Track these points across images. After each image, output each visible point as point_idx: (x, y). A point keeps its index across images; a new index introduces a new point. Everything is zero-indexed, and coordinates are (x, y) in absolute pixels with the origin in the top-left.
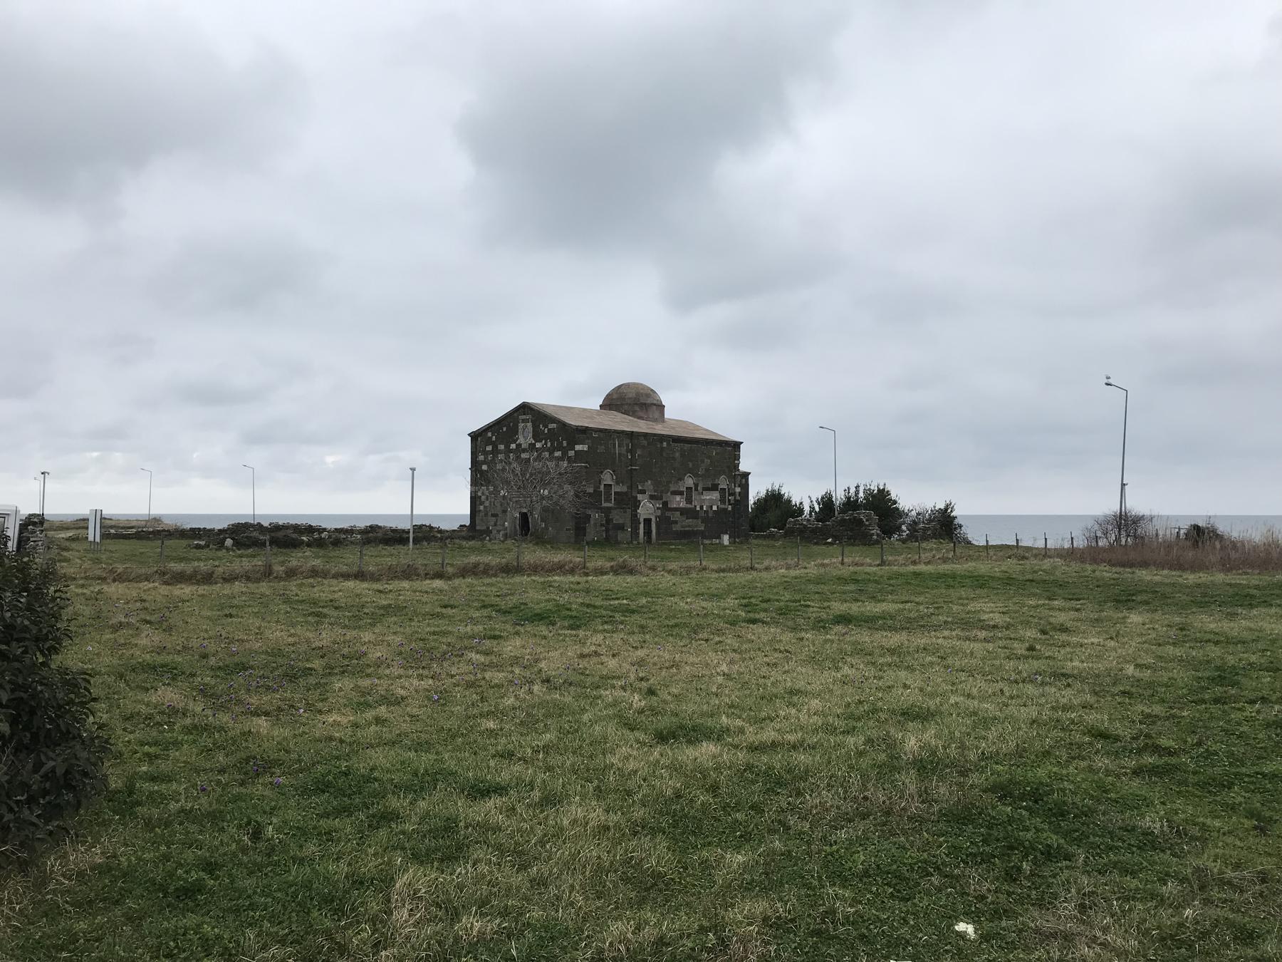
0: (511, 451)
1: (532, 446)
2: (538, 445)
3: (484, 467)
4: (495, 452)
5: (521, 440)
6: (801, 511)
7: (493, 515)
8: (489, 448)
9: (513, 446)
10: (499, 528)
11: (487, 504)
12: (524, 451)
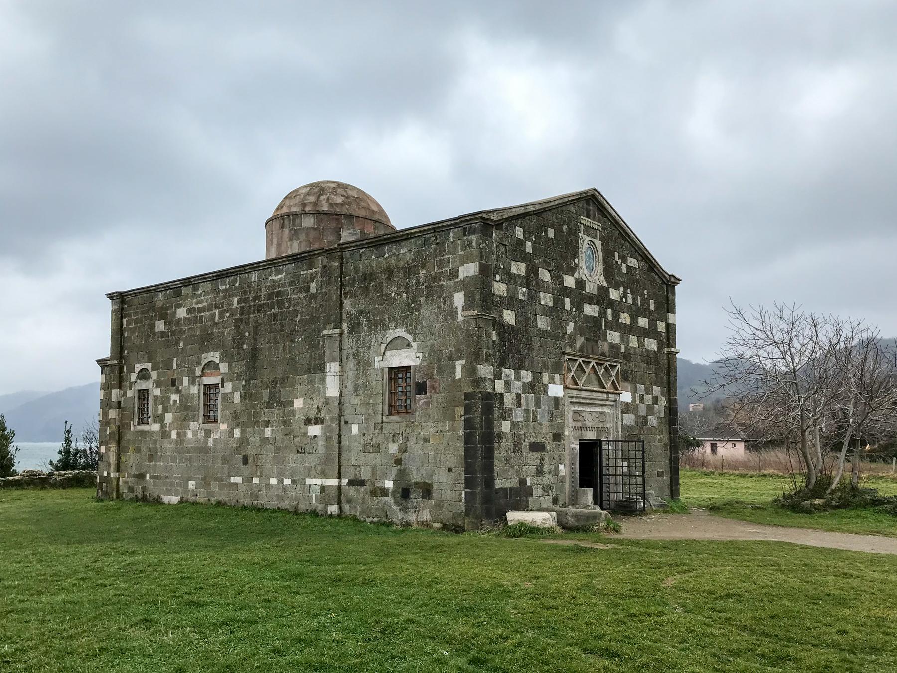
0: (566, 291)
1: (603, 292)
2: (614, 295)
3: (509, 317)
4: (531, 280)
7: (537, 447)
8: (519, 268)
9: (569, 281)
10: (546, 479)
11: (519, 415)
12: (590, 299)
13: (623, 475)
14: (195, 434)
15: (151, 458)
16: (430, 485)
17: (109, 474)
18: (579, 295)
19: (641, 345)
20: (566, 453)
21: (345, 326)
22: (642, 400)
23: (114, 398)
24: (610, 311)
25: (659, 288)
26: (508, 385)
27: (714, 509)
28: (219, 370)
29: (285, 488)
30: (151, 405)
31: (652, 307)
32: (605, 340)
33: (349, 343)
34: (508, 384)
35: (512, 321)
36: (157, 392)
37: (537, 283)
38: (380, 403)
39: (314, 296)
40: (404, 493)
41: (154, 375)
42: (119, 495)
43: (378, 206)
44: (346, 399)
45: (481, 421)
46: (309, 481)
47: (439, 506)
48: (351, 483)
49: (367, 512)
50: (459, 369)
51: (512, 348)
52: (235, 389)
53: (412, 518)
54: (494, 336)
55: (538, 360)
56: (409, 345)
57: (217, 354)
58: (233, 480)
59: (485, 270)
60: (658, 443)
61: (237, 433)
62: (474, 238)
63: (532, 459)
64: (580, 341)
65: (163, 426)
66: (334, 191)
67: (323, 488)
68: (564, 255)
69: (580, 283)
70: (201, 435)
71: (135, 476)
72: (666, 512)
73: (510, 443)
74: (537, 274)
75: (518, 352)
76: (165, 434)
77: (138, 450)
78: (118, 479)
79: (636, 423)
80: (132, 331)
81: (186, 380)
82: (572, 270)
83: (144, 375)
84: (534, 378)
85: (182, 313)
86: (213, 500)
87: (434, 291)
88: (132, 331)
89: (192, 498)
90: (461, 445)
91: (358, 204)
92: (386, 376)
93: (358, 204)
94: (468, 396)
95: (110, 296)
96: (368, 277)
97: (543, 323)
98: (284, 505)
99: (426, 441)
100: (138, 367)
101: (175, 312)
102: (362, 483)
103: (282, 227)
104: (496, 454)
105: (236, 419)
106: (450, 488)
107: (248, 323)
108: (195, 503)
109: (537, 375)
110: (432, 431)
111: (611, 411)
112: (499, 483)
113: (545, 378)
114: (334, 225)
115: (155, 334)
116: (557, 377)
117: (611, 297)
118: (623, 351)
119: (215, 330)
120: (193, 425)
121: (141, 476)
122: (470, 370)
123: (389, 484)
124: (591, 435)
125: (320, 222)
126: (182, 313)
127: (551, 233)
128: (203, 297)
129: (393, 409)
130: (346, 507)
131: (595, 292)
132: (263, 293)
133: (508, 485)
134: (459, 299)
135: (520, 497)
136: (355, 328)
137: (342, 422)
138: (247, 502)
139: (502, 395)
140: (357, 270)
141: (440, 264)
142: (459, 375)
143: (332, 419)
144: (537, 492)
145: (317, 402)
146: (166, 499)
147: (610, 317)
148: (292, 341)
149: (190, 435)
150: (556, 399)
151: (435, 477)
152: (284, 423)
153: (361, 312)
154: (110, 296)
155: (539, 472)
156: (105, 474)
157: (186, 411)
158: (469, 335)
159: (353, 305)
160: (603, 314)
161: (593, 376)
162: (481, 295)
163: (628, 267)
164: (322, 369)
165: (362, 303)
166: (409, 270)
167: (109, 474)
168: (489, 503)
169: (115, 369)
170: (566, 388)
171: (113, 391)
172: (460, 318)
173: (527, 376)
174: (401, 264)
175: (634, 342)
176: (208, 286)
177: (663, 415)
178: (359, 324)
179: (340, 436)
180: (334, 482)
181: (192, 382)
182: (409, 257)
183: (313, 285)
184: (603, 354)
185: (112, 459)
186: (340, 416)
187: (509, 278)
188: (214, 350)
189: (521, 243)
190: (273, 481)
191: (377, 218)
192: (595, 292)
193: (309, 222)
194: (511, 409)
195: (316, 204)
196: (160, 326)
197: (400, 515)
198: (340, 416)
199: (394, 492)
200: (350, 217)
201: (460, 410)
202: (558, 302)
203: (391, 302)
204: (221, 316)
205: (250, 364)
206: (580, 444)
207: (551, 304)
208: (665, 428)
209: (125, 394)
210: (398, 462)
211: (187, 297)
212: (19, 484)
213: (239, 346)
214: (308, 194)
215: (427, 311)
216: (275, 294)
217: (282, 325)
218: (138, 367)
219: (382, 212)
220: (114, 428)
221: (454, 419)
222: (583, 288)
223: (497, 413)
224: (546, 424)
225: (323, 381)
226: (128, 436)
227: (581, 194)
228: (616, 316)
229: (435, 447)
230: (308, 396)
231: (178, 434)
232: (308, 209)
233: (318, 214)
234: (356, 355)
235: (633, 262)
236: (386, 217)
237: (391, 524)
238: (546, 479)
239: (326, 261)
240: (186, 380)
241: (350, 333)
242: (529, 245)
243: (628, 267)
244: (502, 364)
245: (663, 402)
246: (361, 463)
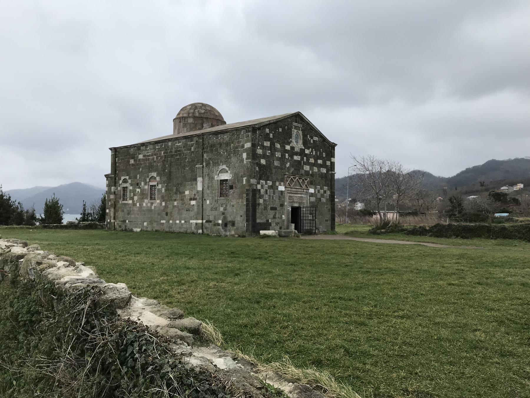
0: (287, 151)
1: (302, 151)
2: (307, 152)
3: (263, 162)
4: (272, 148)
5: (294, 144)
6: (32, 217)
7: (273, 209)
8: (267, 144)
9: (288, 147)
10: (277, 220)
11: (266, 197)
12: (297, 154)
13: (310, 220)
14: (147, 204)
15: (129, 214)
16: (234, 222)
17: (110, 221)
18: (292, 152)
19: (319, 170)
20: (286, 211)
21: (204, 164)
22: (319, 192)
23: (112, 190)
24: (305, 158)
25: (327, 148)
26: (262, 186)
27: (346, 234)
28: (156, 179)
29: (182, 224)
30: (128, 193)
31: (324, 156)
32: (303, 169)
33: (206, 170)
34: (263, 186)
35: (264, 163)
36: (131, 188)
37: (275, 149)
38: (217, 192)
39: (193, 152)
40: (225, 225)
41: (130, 181)
42: (115, 229)
43: (218, 113)
44: (204, 191)
45: (252, 198)
46: (191, 221)
47: (237, 229)
48: (207, 222)
49: (212, 232)
50: (244, 181)
51: (264, 173)
52: (162, 187)
53: (228, 233)
54: (257, 169)
55: (274, 177)
56: (227, 172)
57: (156, 173)
58: (162, 222)
59: (254, 145)
60: (326, 209)
61: (164, 204)
62: (249, 133)
63: (271, 213)
64: (292, 170)
65: (133, 201)
66: (201, 108)
67: (196, 224)
68: (286, 137)
69: (293, 148)
70: (149, 205)
71: (122, 221)
72: (325, 234)
73: (263, 207)
74: (274, 145)
75: (266, 174)
76: (134, 204)
77: (123, 211)
78: (114, 223)
79: (316, 201)
80: (120, 163)
81: (143, 183)
82: (289, 143)
83: (125, 181)
84: (272, 183)
85: (141, 157)
86: (154, 230)
87: (236, 152)
88: (120, 163)
89: (145, 229)
90: (245, 207)
91: (210, 113)
92: (219, 183)
93: (210, 113)
94: (247, 190)
95: (111, 149)
96: (213, 146)
97: (276, 163)
98: (182, 230)
99: (233, 206)
100: (123, 178)
101: (138, 157)
102: (211, 222)
103: (180, 122)
104: (257, 211)
105: (163, 199)
106: (241, 222)
107: (167, 162)
108: (146, 231)
109: (274, 183)
110: (235, 203)
111: (306, 195)
112: (258, 221)
113: (277, 183)
114: (200, 122)
115: (130, 165)
116: (282, 183)
117: (306, 152)
118: (311, 173)
119: (155, 164)
120: (146, 201)
121: (124, 221)
122: (248, 181)
123: (220, 222)
124: (296, 205)
125: (195, 120)
126: (141, 157)
127: (280, 130)
128: (150, 151)
129: (221, 195)
130: (205, 231)
131: (299, 151)
132: (173, 150)
133: (262, 222)
134: (245, 155)
135: (267, 226)
136: (208, 165)
137: (203, 200)
138: (167, 230)
140: (208, 142)
141: (238, 142)
142: (244, 183)
143: (199, 199)
144: (273, 225)
145: (194, 192)
146: (135, 230)
147: (305, 160)
148: (185, 169)
149: (144, 205)
150: (282, 191)
151: (236, 219)
152: (182, 200)
153: (210, 159)
154: (111, 149)
155: (274, 217)
156: (109, 221)
157: (143, 195)
158: (248, 169)
159: (207, 156)
160: (302, 159)
161: (297, 183)
162: (253, 155)
163: (314, 141)
164: (196, 180)
165: (210, 155)
166: (228, 144)
167: (110, 221)
168: (255, 227)
169: (113, 179)
170: (285, 187)
171: (112, 188)
172: (245, 162)
173: (270, 183)
174: (225, 142)
175: (316, 169)
176: (151, 147)
177: (328, 198)
178: (209, 163)
179: (202, 205)
180: (200, 221)
181: (145, 184)
182: (227, 139)
183: (193, 148)
184: (302, 175)
185: (112, 215)
186: (203, 197)
187: (263, 147)
188: (155, 172)
189: (268, 134)
190: (178, 222)
191: (218, 119)
192: (299, 151)
193: (191, 120)
195: (193, 113)
196: (132, 161)
197: (224, 233)
198: (203, 197)
199: (222, 224)
200: (207, 118)
201: (245, 195)
202: (283, 156)
203: (221, 155)
204: (157, 158)
205: (168, 178)
206: (292, 208)
207: (280, 156)
208: (329, 203)
209: (117, 189)
210: (223, 214)
211: (143, 150)
212: (66, 227)
213: (164, 171)
214: (190, 109)
215: (234, 159)
216: (178, 151)
217: (181, 163)
218: (123, 178)
219: (220, 115)
220: (113, 202)
221: (242, 198)
222: (294, 150)
223: (258, 196)
224: (277, 200)
225: (196, 184)
226: (118, 206)
227: (293, 114)
228: (308, 160)
229: (236, 208)
230: (191, 190)
231: (140, 204)
232: (190, 115)
233: (194, 117)
234: (208, 175)
235: (316, 139)
236: (222, 118)
237: (221, 236)
238: (277, 220)
239: (197, 139)
240: (143, 183)
241: (206, 166)
242: (271, 135)
243: (314, 141)
244: (260, 179)
245: (328, 193)
246: (210, 214)
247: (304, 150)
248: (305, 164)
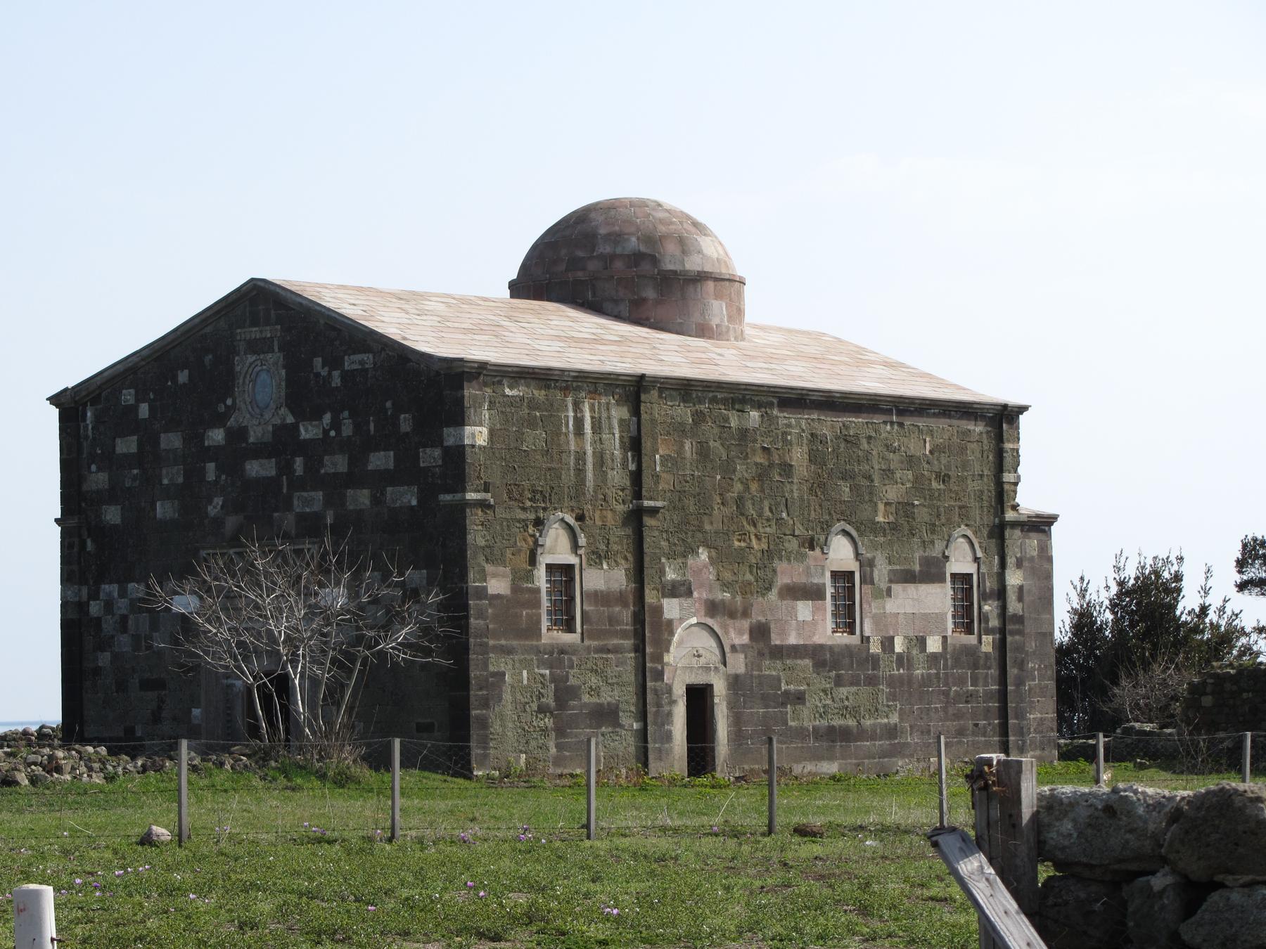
0: (213, 453)
2: (308, 432)
3: (112, 515)
4: (149, 456)
8: (127, 445)
9: (217, 436)
12: (259, 451)
26: (109, 606)
64: (231, 522)
69: (237, 435)
82: (219, 420)
139: (99, 619)
194: (113, 637)
243: (345, 376)
247: (295, 427)
248: (299, 484)
